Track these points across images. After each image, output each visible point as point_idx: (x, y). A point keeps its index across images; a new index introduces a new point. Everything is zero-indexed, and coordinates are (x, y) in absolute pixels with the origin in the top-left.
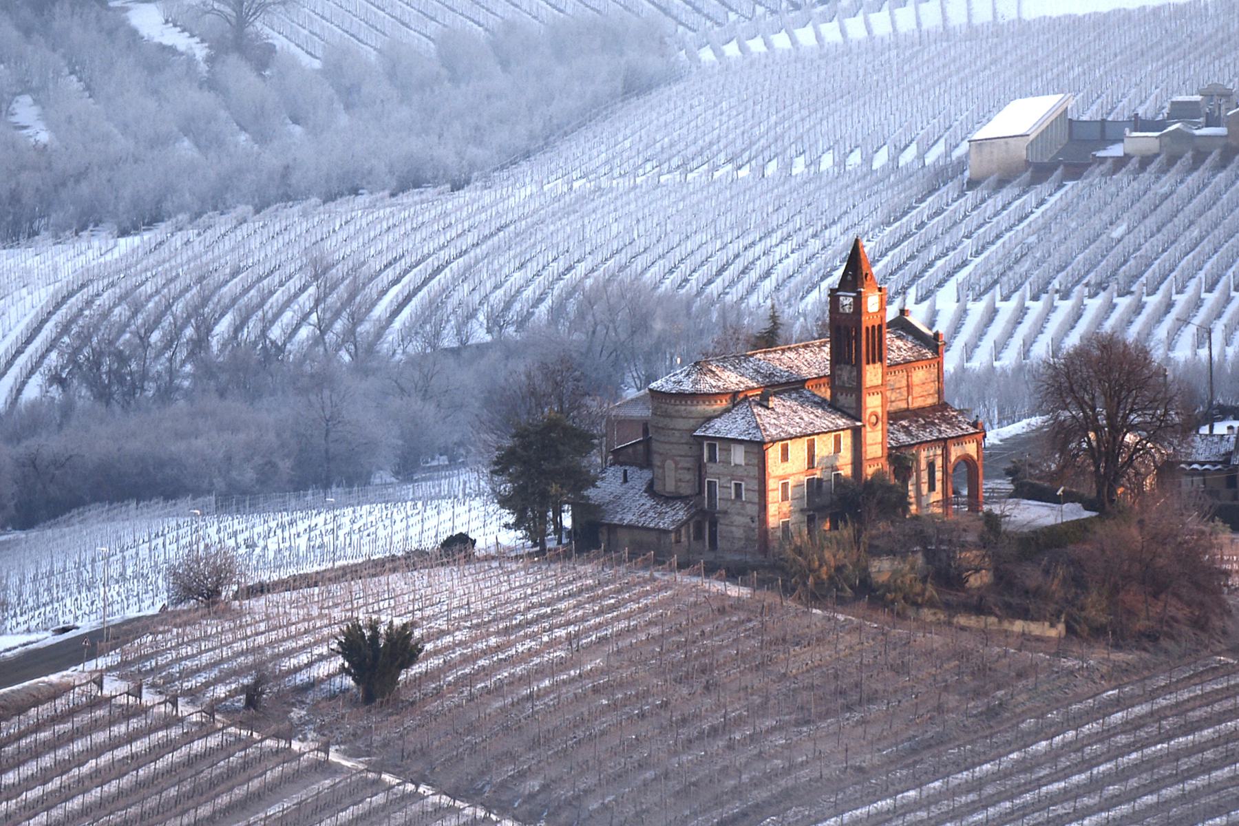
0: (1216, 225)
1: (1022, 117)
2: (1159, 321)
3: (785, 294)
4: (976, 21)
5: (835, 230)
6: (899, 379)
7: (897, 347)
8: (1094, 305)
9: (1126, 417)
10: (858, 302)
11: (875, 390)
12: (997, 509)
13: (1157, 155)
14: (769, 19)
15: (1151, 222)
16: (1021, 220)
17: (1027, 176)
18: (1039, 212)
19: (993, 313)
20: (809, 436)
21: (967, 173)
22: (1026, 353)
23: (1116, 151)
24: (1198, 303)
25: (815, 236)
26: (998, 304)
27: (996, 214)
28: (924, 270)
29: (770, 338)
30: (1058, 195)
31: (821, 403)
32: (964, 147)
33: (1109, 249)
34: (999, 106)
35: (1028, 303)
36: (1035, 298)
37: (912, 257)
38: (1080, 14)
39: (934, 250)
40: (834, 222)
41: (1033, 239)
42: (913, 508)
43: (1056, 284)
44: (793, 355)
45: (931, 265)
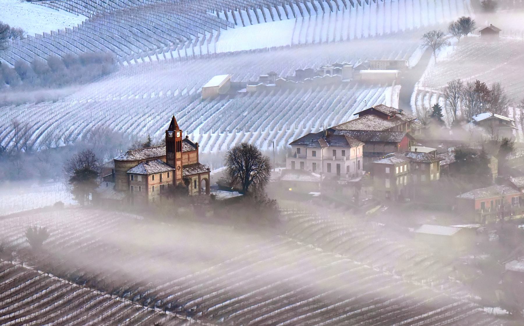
0: (273, 112)
1: (217, 81)
2: (258, 139)
3: (150, 132)
4: (203, 54)
5: (164, 113)
6: (185, 156)
7: (185, 147)
8: (239, 135)
9: (251, 167)
10: (174, 134)
11: (179, 159)
12: (214, 194)
13: (256, 92)
14: (143, 53)
15: (254, 111)
16: (217, 110)
17: (218, 98)
18: (222, 108)
19: (210, 137)
20: (160, 173)
21: (201, 97)
22: (220, 149)
23: (244, 91)
24: (268, 134)
25: (158, 115)
26: (211, 135)
27: (210, 109)
28: (190, 125)
29: (147, 145)
30: (228, 103)
31: (164, 163)
32: (200, 90)
33: (243, 119)
34: (211, 77)
35: (220, 134)
36: (222, 133)
37: (186, 121)
38: (233, 51)
39: (193, 119)
40: (163, 111)
41: (221, 116)
42: (190, 193)
43: (228, 129)
44: (155, 150)
45: (192, 123)
